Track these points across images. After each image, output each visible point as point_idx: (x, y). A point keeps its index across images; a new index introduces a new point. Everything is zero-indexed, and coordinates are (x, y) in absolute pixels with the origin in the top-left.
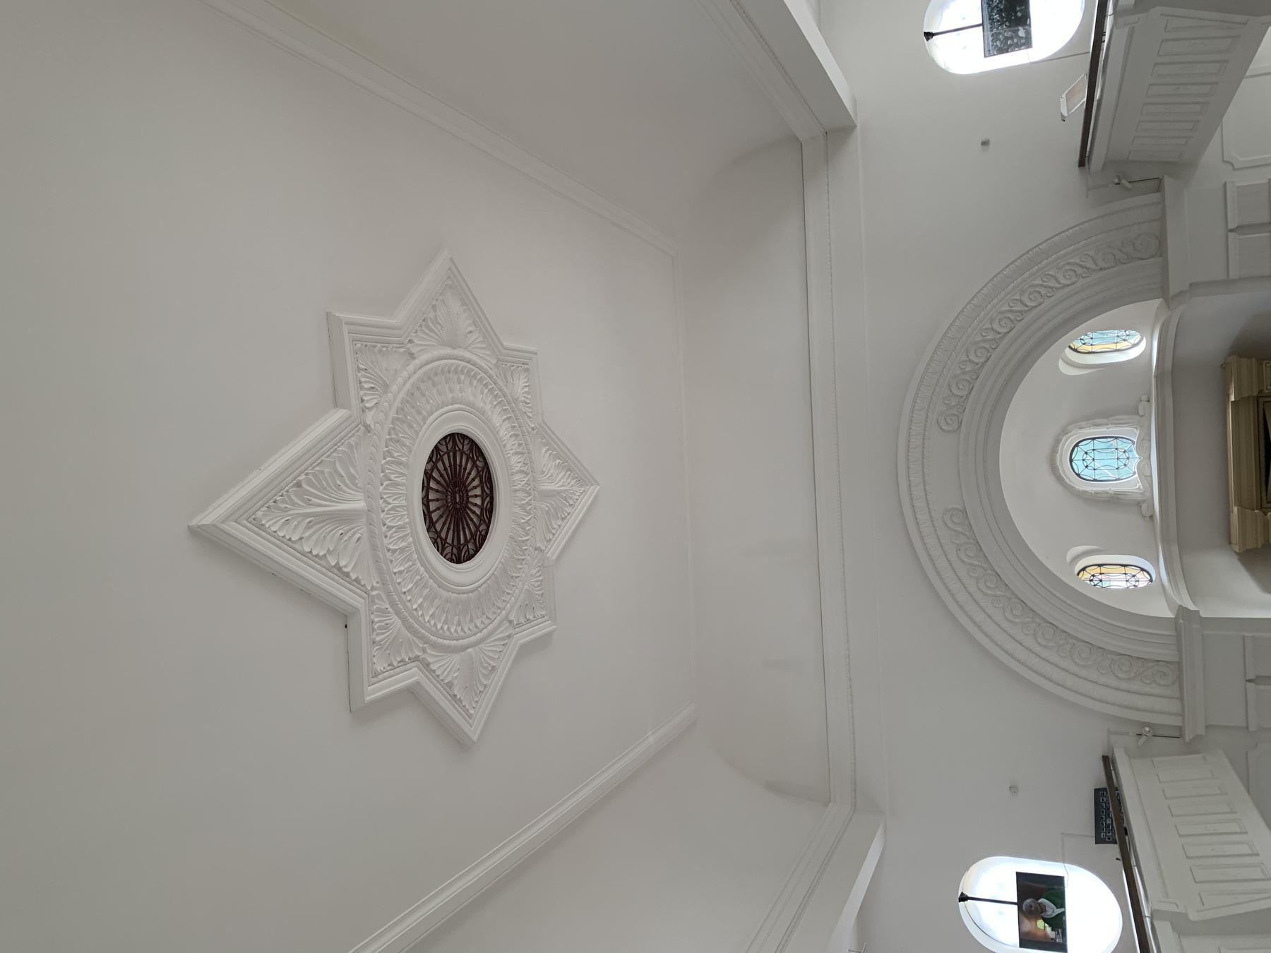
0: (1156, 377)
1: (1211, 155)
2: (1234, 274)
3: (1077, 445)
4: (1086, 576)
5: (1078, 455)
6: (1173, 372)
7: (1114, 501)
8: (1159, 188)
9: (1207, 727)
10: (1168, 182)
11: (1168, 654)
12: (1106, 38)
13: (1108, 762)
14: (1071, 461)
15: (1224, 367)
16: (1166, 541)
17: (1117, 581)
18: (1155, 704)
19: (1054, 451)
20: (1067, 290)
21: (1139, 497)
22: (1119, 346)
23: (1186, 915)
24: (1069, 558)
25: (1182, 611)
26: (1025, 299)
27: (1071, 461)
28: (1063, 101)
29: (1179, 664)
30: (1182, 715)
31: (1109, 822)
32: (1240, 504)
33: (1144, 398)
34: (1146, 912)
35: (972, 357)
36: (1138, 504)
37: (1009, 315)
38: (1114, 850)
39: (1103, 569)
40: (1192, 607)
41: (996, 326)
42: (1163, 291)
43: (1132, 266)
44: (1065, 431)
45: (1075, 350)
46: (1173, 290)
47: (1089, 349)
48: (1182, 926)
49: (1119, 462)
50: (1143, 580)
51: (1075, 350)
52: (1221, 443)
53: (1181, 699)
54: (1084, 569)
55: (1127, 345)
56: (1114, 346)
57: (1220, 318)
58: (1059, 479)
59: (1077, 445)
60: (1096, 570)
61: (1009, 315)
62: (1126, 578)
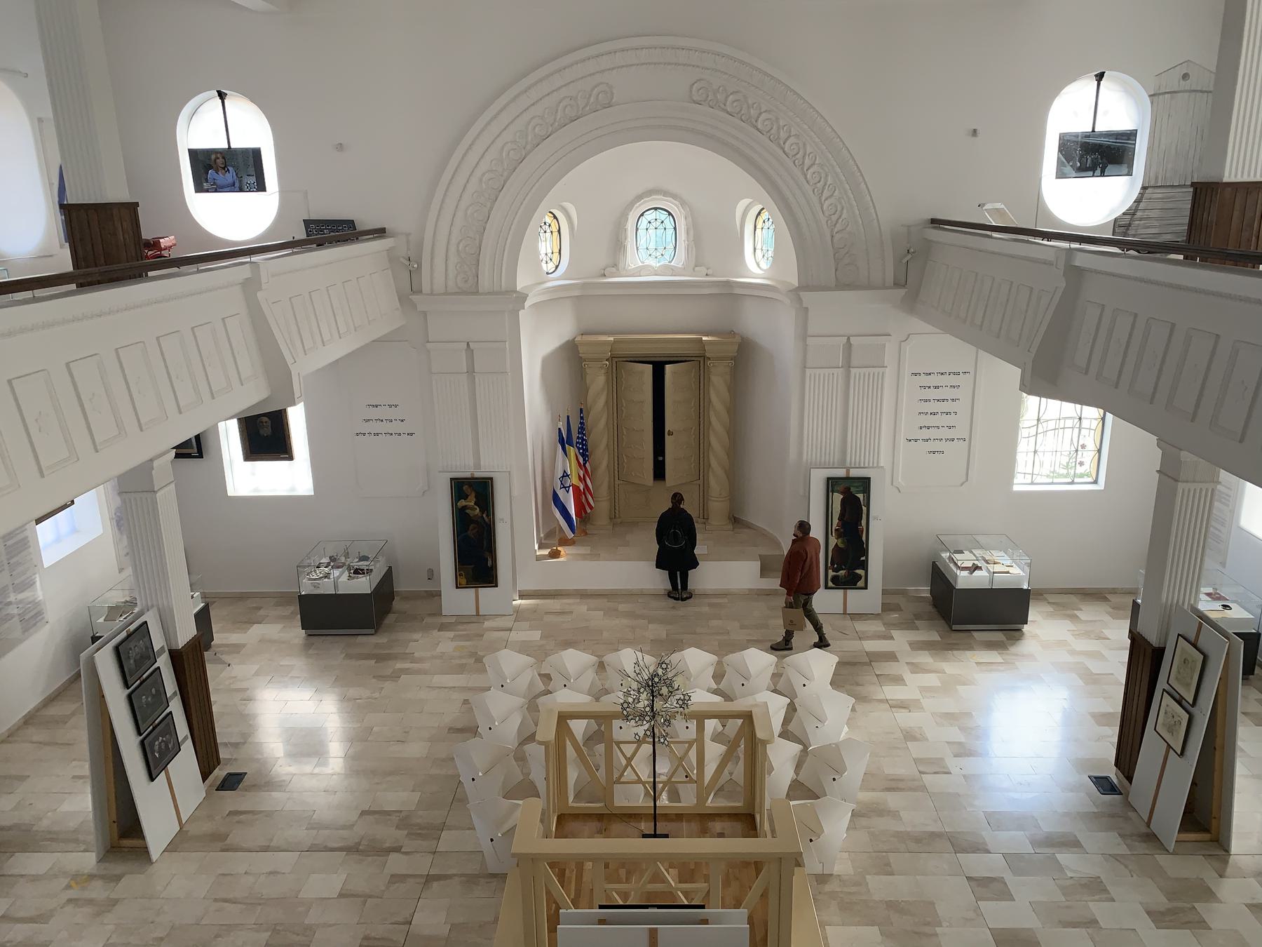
0: (728, 282)
1: (916, 324)
2: (810, 341)
3: (670, 214)
4: (548, 219)
5: (663, 215)
6: (731, 295)
7: (618, 245)
8: (897, 285)
9: (425, 314)
10: (902, 292)
11: (485, 283)
12: (1045, 242)
13: (380, 233)
14: (656, 209)
15: (732, 333)
16: (584, 286)
17: (546, 245)
18: (439, 272)
19: (666, 193)
20: (819, 209)
21: (621, 265)
22: (758, 252)
23: (260, 289)
24: (565, 204)
25: (523, 298)
26: (815, 168)
27: (656, 209)
28: (999, 205)
29: (477, 293)
30: (432, 294)
31: (327, 232)
32: (615, 342)
33: (710, 272)
34: (255, 258)
35: (764, 116)
36: (615, 265)
37: (801, 153)
38: (301, 234)
39: (556, 234)
40: (527, 304)
41: (792, 140)
42: (804, 287)
43: (833, 262)
44: (683, 203)
45: (759, 214)
46: (807, 296)
47: (759, 225)
48: (250, 287)
49: (654, 250)
50: (551, 267)
51: (759, 214)
52: (668, 326)
53: (446, 293)
54: (555, 217)
55: (760, 255)
56: (759, 247)
57: (775, 332)
58: (639, 198)
59: (670, 214)
60: (555, 228)
61: (801, 153)
62: (548, 254)
